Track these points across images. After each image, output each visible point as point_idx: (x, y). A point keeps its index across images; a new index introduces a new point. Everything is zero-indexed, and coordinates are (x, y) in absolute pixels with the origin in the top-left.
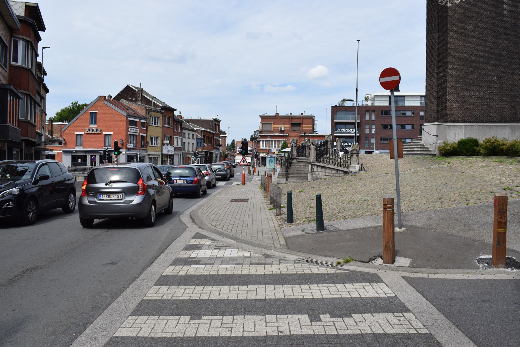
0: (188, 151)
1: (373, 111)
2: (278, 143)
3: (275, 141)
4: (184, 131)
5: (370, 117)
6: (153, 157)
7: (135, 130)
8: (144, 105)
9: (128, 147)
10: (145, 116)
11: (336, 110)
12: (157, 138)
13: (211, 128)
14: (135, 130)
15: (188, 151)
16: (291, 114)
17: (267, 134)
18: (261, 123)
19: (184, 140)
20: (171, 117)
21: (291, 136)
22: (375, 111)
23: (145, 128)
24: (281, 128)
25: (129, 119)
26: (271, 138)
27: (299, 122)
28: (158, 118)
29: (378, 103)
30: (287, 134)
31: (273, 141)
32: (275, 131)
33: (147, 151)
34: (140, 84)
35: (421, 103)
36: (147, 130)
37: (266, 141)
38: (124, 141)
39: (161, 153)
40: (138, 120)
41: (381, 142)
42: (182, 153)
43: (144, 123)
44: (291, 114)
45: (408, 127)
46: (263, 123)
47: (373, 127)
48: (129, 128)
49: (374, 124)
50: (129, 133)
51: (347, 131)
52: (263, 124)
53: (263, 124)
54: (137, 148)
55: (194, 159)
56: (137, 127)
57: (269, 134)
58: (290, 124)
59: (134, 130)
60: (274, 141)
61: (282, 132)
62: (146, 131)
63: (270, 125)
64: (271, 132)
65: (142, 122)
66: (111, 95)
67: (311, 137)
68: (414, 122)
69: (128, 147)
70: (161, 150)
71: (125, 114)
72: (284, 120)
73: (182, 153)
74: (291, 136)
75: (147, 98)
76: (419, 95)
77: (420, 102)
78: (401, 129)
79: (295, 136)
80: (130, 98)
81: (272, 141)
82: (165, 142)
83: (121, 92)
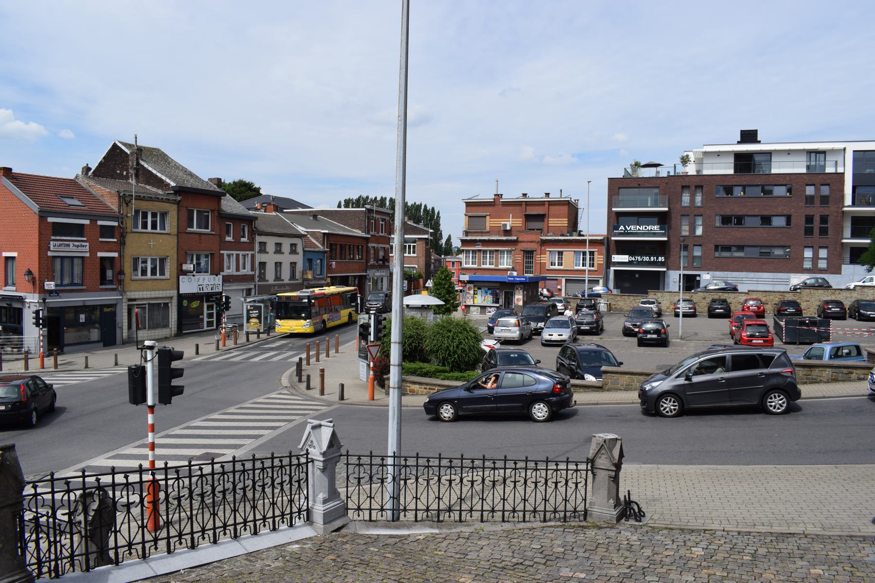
0: (278, 278)
1: (697, 187)
2: (497, 256)
4: (259, 239)
5: (692, 200)
6: (149, 304)
7: (75, 246)
8: (142, 185)
9: (46, 288)
10: (116, 209)
11: (616, 186)
12: (163, 261)
13: (362, 228)
14: (75, 246)
15: (278, 278)
16: (547, 195)
17: (474, 238)
18: (466, 215)
19: (260, 258)
20: (211, 210)
21: (523, 242)
22: (702, 187)
23: (115, 240)
24: (504, 225)
25: (51, 220)
26: (483, 246)
27: (541, 213)
28: (164, 215)
29: (711, 169)
30: (515, 238)
31: (486, 251)
32: (493, 231)
33: (123, 292)
34: (136, 138)
35: (808, 167)
37: (473, 251)
38: (36, 274)
39: (176, 292)
40: (87, 222)
41: (717, 254)
42: (253, 286)
43: (113, 227)
44: (547, 195)
45: (779, 222)
46: (470, 214)
47: (699, 221)
48: (52, 243)
49: (702, 215)
50: (50, 254)
51: (639, 230)
52: (469, 217)
53: (469, 217)
54: (84, 287)
55: (251, 306)
56: (85, 239)
57: (478, 238)
58: (524, 217)
59: (68, 245)
60: (490, 251)
61: (507, 232)
62: (121, 245)
63: (484, 218)
64: (482, 233)
65: (101, 226)
66: (89, 166)
68: (793, 210)
69: (46, 288)
70: (175, 286)
71: (35, 208)
72: (510, 208)
73: (253, 286)
74: (523, 242)
75: (148, 170)
76: (804, 150)
77: (805, 164)
78: (761, 225)
79: (532, 242)
80: (118, 172)
81: (485, 252)
82: (185, 267)
83: (104, 158)
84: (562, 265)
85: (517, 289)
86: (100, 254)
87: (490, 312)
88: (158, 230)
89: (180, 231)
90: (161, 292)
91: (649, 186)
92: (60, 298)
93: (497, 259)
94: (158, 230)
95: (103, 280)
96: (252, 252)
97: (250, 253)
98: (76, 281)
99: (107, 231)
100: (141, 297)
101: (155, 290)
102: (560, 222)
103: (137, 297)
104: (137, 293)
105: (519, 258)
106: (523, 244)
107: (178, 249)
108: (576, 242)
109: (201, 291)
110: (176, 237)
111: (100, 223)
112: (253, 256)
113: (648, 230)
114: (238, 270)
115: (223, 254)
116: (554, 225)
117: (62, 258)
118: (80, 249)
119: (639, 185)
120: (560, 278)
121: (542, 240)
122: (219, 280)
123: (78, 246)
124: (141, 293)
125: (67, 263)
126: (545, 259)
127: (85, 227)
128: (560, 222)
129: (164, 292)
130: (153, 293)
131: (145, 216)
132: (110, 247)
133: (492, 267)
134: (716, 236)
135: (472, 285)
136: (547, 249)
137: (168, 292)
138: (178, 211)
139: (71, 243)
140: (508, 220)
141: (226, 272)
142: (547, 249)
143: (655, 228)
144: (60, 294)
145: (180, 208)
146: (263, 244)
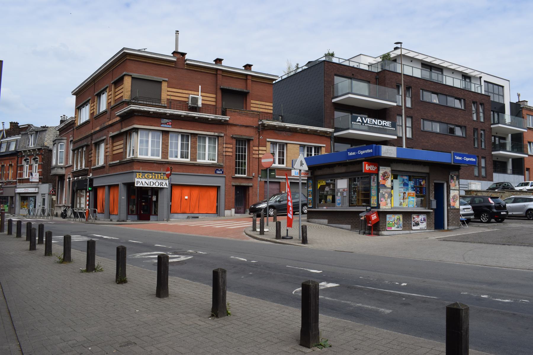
3: (185, 136)
21: (235, 125)
24: (193, 98)
27: (245, 90)
32: (171, 104)
51: (374, 124)
52: (133, 78)
67: (289, 133)
74: (235, 125)
79: (247, 126)
84: (283, 163)
85: (452, 178)
87: (417, 224)
91: (362, 78)
93: (194, 148)
102: (264, 107)
105: (230, 150)
106: (235, 128)
108: (302, 133)
113: (382, 125)
116: (256, 109)
119: (353, 74)
120: (284, 181)
121: (263, 125)
126: (264, 152)
128: (264, 107)
133: (188, 160)
134: (423, 140)
135: (388, 170)
136: (268, 140)
140: (196, 93)
142: (268, 140)
143: (388, 124)
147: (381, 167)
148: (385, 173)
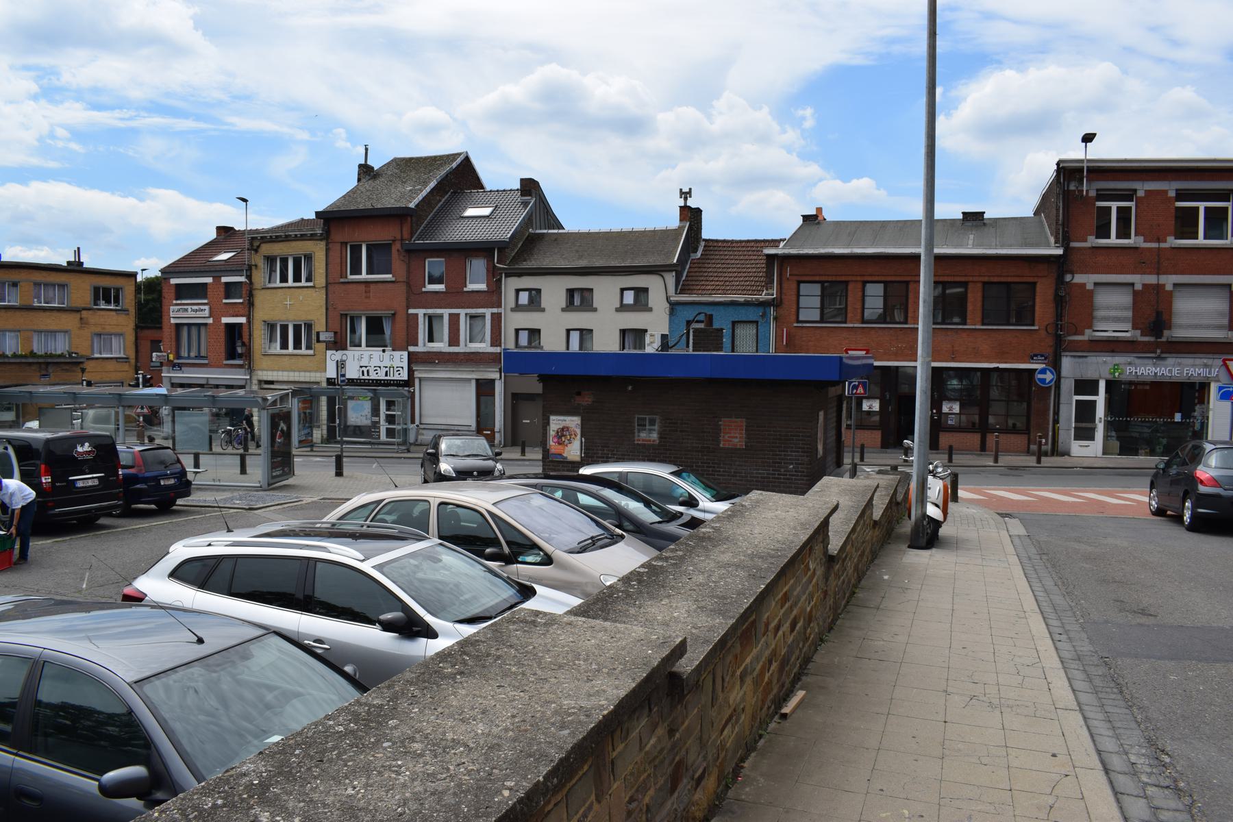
7: (193, 310)
14: (193, 310)
23: (241, 301)
33: (251, 370)
36: (251, 304)
40: (209, 280)
56: (206, 301)
59: (186, 310)
86: (225, 320)
88: (303, 283)
89: (331, 280)
90: (302, 374)
92: (183, 373)
94: (290, 282)
95: (231, 354)
96: (495, 310)
97: (488, 312)
98: (202, 354)
99: (230, 289)
100: (281, 379)
101: (294, 371)
103: (274, 379)
104: (270, 373)
107: (327, 309)
109: (366, 377)
110: (324, 291)
111: (224, 279)
112: (497, 319)
114: (454, 341)
115: (417, 315)
117: (189, 325)
118: (199, 314)
122: (399, 360)
123: (196, 311)
124: (275, 373)
125: (194, 331)
127: (208, 287)
129: (308, 374)
130: (292, 374)
131: (284, 261)
132: (236, 310)
137: (313, 374)
138: (327, 250)
139: (189, 307)
141: (423, 346)
144: (183, 368)
145: (331, 245)
146: (535, 294)
147: (552, 418)
148: (563, 429)
